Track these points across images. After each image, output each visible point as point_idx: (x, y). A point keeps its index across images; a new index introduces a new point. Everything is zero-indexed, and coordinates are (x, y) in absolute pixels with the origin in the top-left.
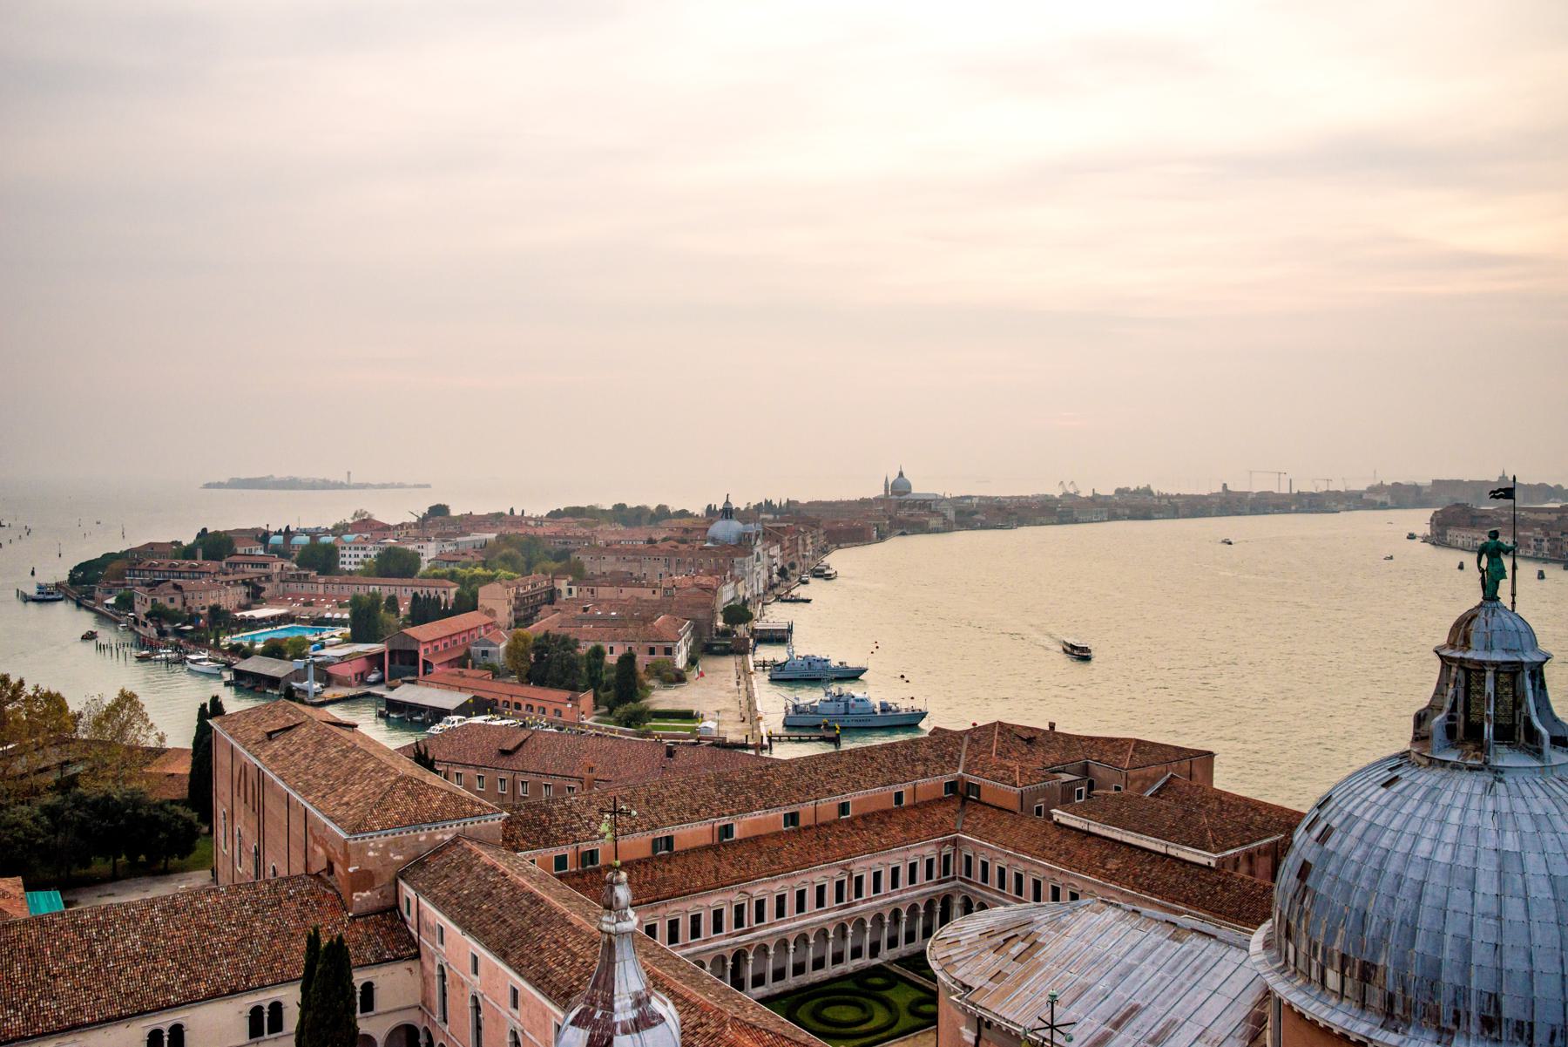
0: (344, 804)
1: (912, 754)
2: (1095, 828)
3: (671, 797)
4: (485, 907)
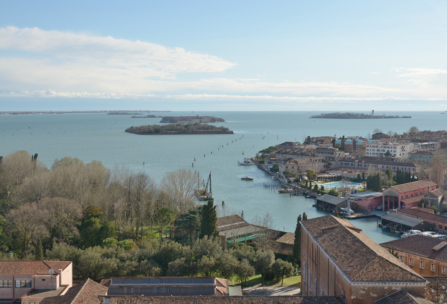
0: (351, 266)
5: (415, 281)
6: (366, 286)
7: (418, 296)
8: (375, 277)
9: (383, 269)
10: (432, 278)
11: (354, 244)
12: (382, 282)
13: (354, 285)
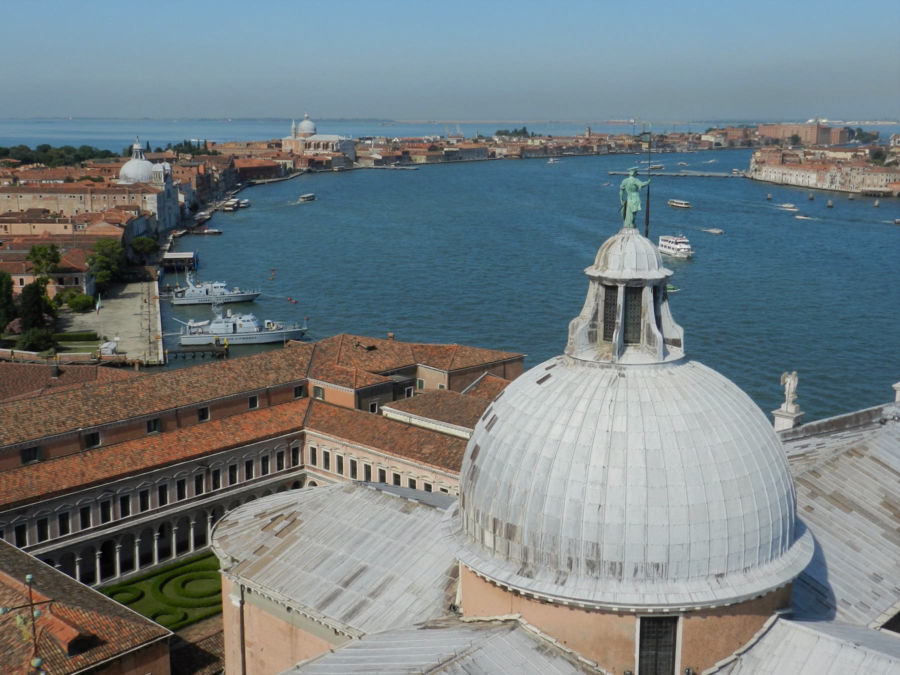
1: (266, 365)
2: (416, 421)
3: (39, 412)
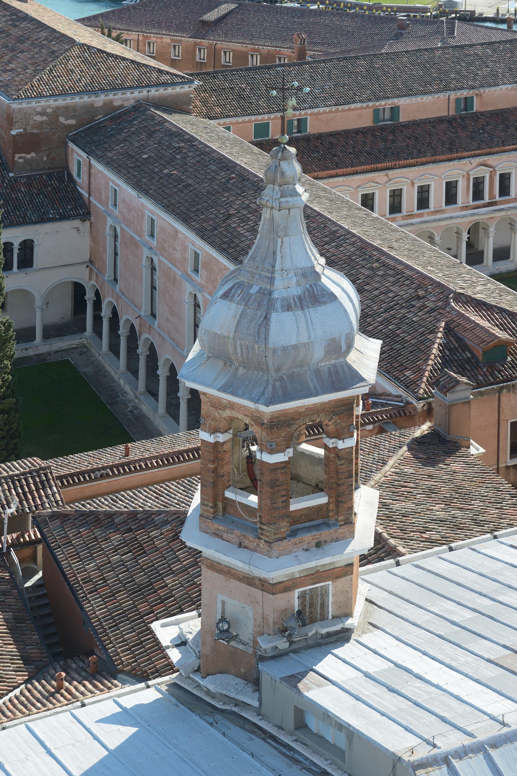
0: (9, 71)
4: (165, 171)
5: (169, 83)
6: (49, 107)
7: (176, 112)
8: (71, 87)
9: (91, 69)
10: (208, 74)
11: (15, 26)
12: (88, 93)
13: (20, 106)
